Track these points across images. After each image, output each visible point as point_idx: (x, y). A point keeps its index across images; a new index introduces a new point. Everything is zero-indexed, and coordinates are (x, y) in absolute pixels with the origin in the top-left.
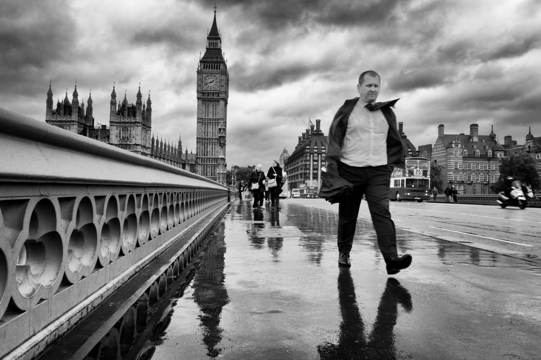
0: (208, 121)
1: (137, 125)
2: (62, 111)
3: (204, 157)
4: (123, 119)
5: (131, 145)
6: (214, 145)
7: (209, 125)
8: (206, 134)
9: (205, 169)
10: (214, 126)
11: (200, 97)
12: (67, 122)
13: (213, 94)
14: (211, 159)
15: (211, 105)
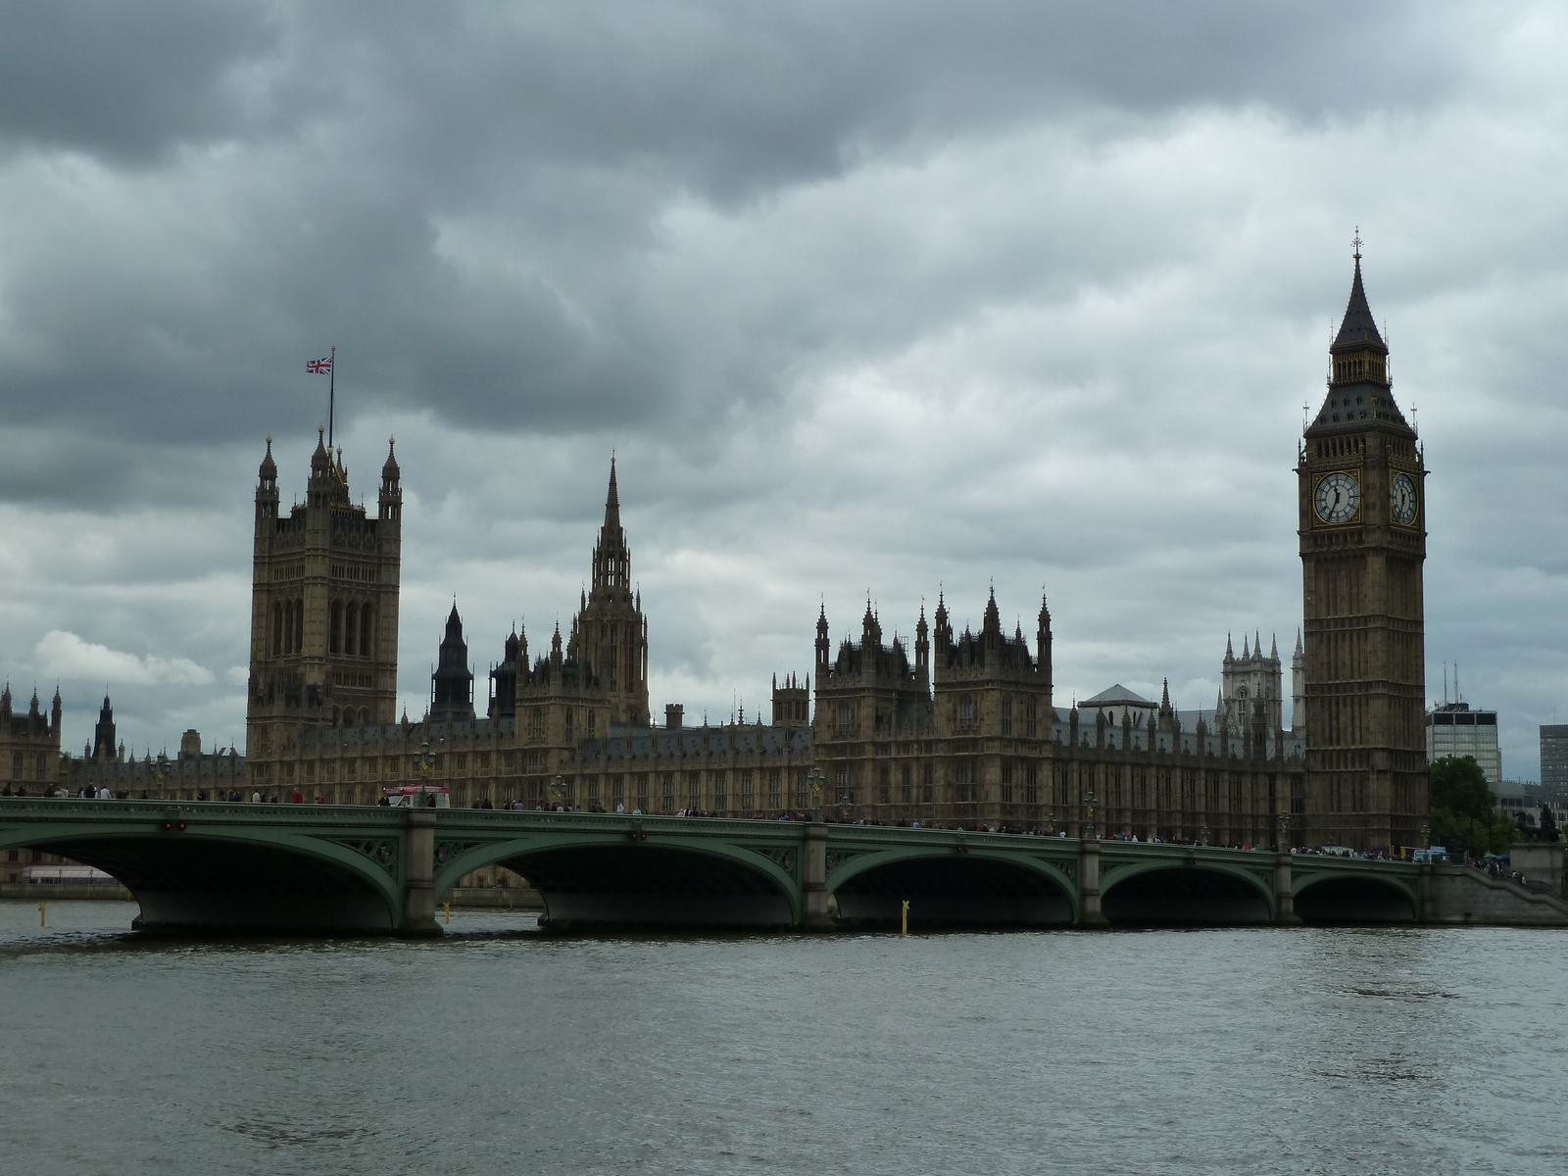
0: (1336, 626)
1: (986, 687)
2: (845, 664)
3: (1331, 748)
4: (961, 675)
5: (976, 739)
6: (1357, 708)
7: (1339, 641)
8: (1333, 672)
9: (1335, 787)
10: (1355, 639)
11: (1309, 551)
12: (851, 691)
13: (1345, 536)
14: (1349, 755)
15: (1343, 573)
